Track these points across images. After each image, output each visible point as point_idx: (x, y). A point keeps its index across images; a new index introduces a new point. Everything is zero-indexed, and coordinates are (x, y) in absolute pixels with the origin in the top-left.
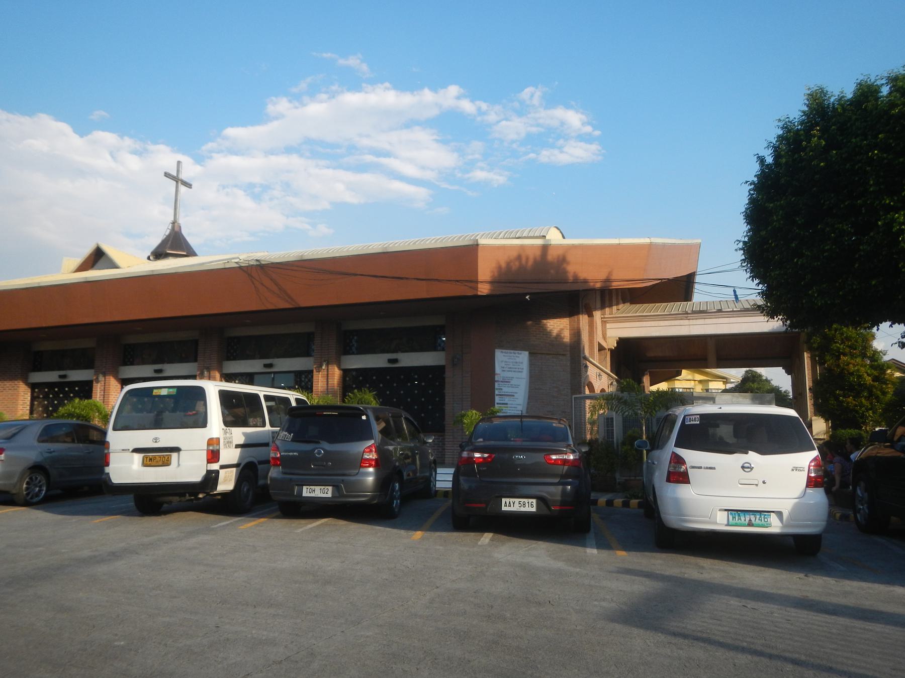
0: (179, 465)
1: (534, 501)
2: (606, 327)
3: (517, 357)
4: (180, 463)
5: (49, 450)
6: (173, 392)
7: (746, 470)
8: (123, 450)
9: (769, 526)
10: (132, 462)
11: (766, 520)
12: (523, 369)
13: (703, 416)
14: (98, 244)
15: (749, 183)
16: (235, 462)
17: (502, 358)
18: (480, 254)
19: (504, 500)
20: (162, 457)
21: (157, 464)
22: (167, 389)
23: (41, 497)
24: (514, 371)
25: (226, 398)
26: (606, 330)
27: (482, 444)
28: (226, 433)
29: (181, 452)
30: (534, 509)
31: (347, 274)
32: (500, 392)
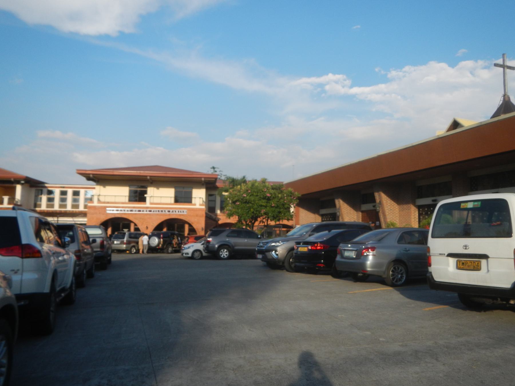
0: (488, 271)
4: (489, 269)
5: (405, 249)
6: (478, 205)
8: (440, 254)
10: (448, 265)
14: (454, 119)
20: (473, 262)
21: (468, 269)
22: (472, 203)
23: (403, 281)
29: (489, 259)
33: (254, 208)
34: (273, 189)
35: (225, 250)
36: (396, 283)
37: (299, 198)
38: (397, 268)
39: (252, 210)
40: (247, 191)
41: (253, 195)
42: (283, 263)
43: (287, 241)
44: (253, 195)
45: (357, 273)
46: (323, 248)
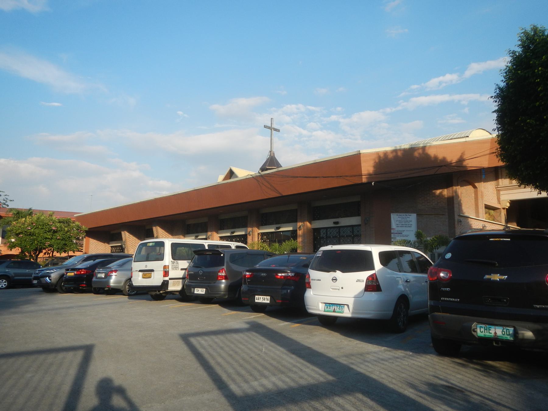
1: (269, 297)
3: (407, 217)
10: (139, 276)
11: (342, 309)
12: (412, 225)
13: (324, 252)
16: (181, 277)
18: (362, 159)
19: (256, 296)
22: (151, 243)
25: (174, 246)
28: (173, 263)
30: (269, 302)
31: (294, 177)
33: (38, 240)
34: (60, 222)
35: (4, 281)
36: (130, 293)
37: (86, 232)
39: (36, 242)
40: (32, 224)
41: (38, 228)
42: (56, 286)
43: (61, 268)
46: (86, 273)
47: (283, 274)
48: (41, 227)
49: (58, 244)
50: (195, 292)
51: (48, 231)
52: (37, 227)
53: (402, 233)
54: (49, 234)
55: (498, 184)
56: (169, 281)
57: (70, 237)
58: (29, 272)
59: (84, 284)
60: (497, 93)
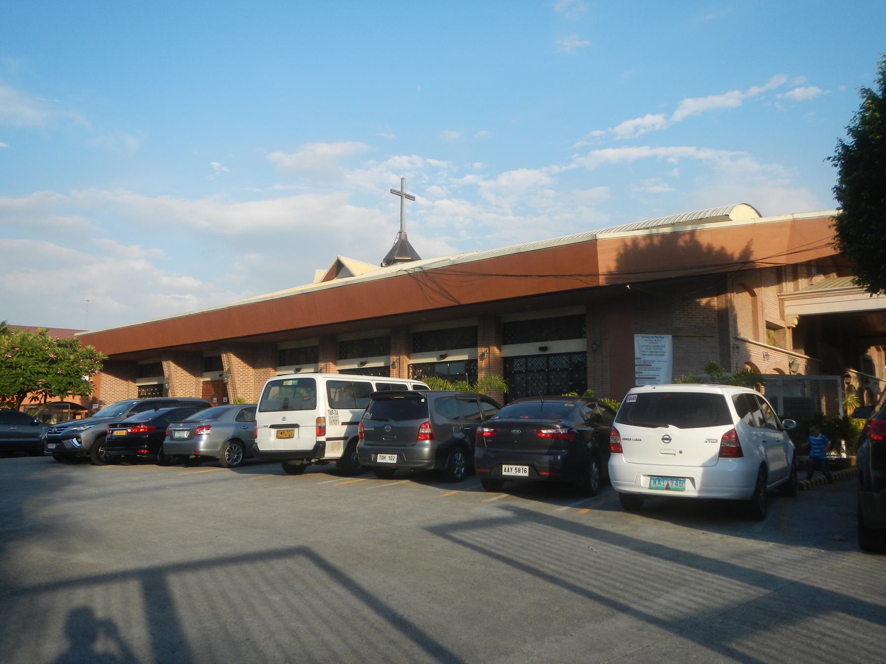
1: (527, 467)
2: (783, 305)
3: (658, 340)
6: (295, 383)
7: (665, 441)
8: (264, 426)
9: (683, 490)
10: (270, 435)
12: (665, 352)
13: (641, 396)
15: (831, 159)
16: (342, 436)
17: (641, 343)
18: (599, 248)
19: (504, 466)
22: (292, 381)
24: (656, 355)
26: (784, 308)
27: (498, 421)
28: (331, 413)
29: (300, 428)
30: (527, 475)
31: (485, 275)
32: (640, 376)
33: (24, 376)
34: (59, 345)
37: (104, 362)
38: (233, 447)
40: (13, 348)
42: (88, 453)
43: (96, 423)
44: (23, 355)
45: (188, 456)
47: (550, 431)
48: (29, 353)
49: (58, 382)
50: (379, 460)
51: (40, 361)
52: (22, 353)
53: (650, 365)
54: (43, 366)
55: (781, 291)
56: (326, 442)
57: (79, 370)
58: (13, 431)
59: (144, 449)
60: (839, 153)
